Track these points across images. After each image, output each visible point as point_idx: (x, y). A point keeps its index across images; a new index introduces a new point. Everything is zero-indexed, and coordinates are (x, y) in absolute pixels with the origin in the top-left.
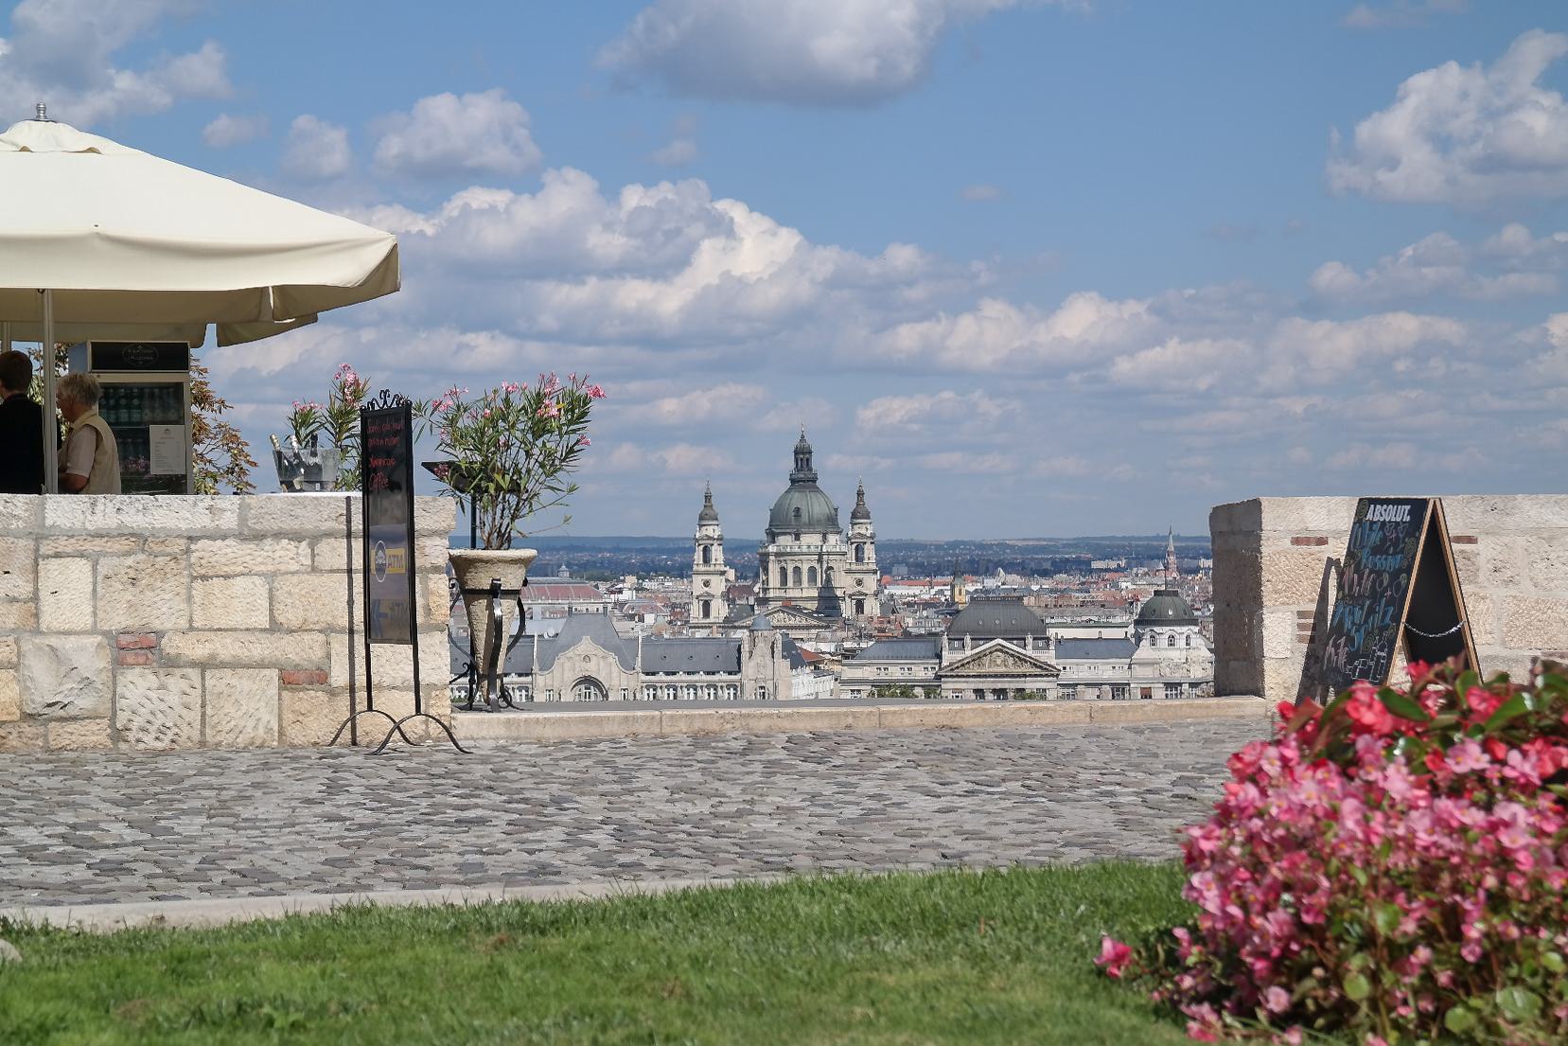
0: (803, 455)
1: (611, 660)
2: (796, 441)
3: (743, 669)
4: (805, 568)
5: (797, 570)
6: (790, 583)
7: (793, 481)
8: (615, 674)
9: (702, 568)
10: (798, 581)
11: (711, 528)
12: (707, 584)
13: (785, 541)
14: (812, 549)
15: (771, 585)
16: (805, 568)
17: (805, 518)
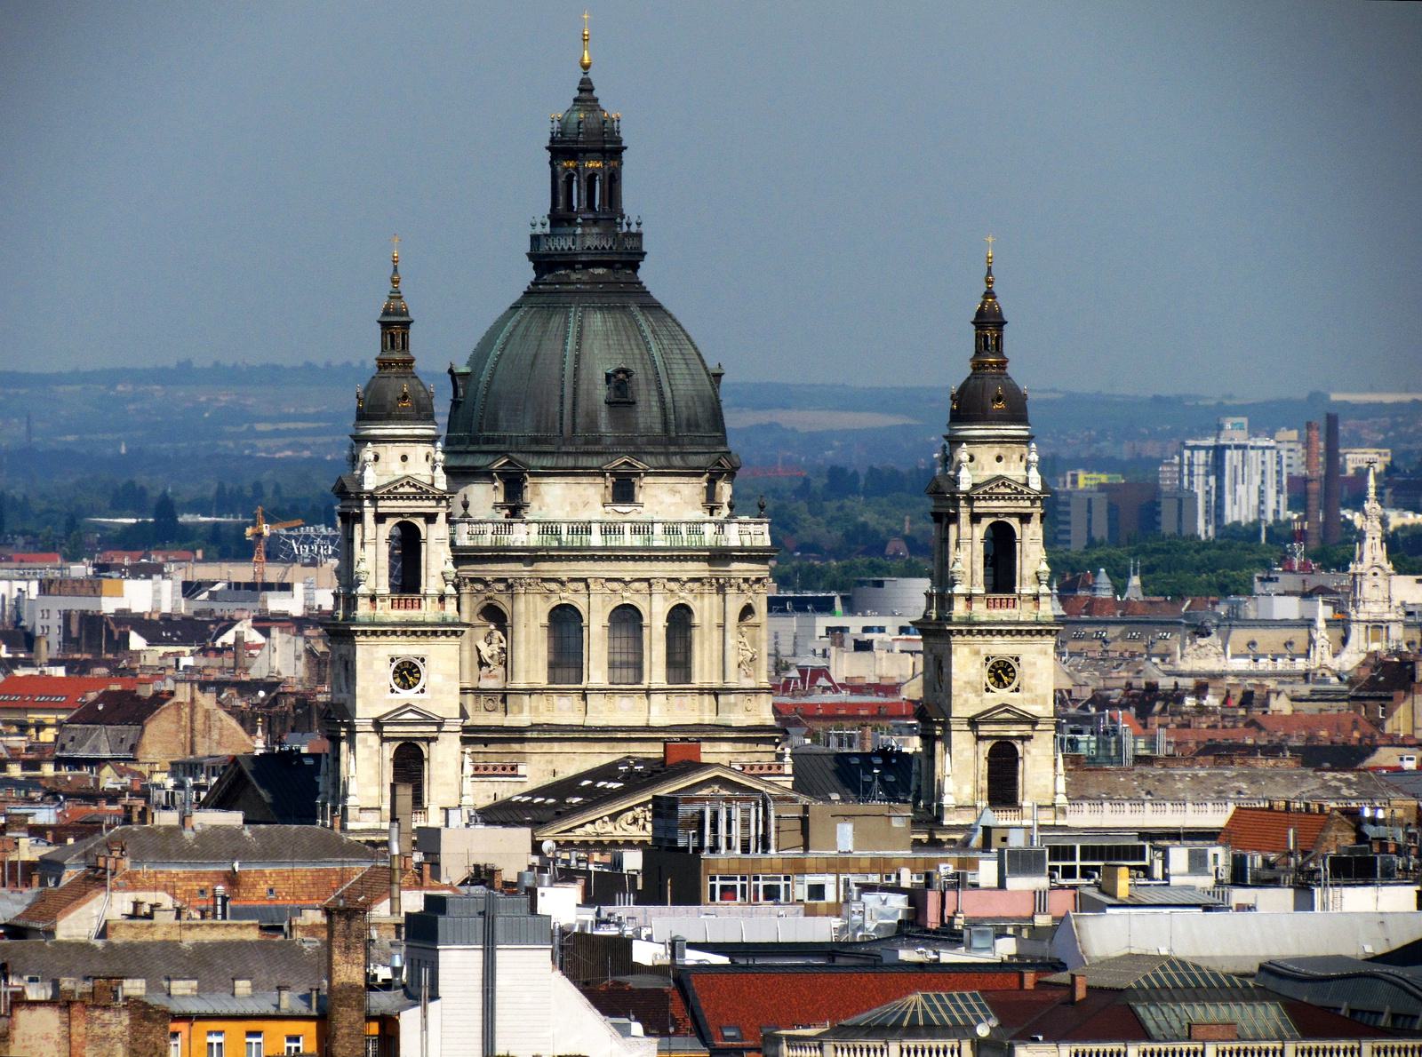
2: (558, 105)
5: (627, 619)
6: (597, 672)
7: (544, 262)
9: (388, 612)
10: (629, 666)
12: (407, 673)
14: (685, 539)
17: (647, 415)
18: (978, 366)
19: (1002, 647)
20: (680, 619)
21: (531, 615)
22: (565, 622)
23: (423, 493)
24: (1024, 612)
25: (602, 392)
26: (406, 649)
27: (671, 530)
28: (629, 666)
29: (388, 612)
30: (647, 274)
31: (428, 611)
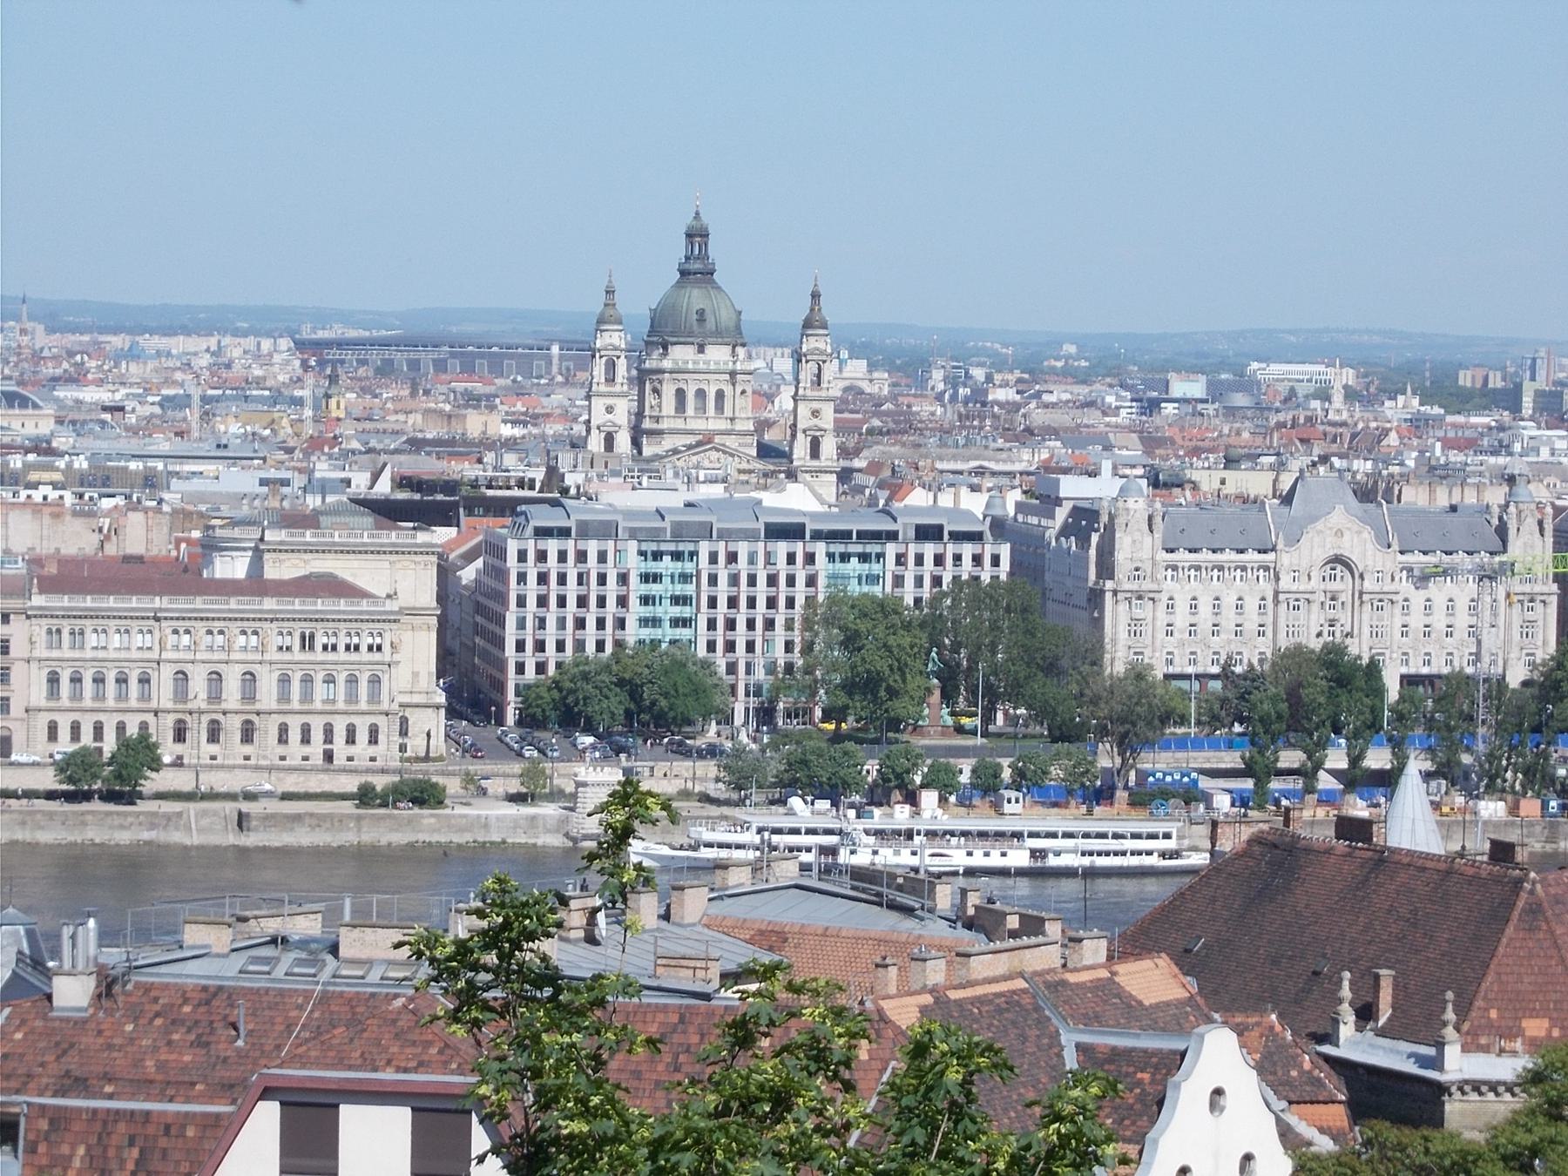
0: (697, 235)
1: (1365, 535)
2: (689, 219)
3: (1510, 548)
5: (701, 394)
6: (690, 411)
7: (684, 273)
8: (1370, 553)
9: (603, 388)
10: (701, 408)
13: (682, 354)
14: (722, 367)
15: (664, 413)
17: (710, 324)
18: (812, 310)
19: (815, 405)
20: (720, 395)
21: (668, 391)
22: (681, 394)
23: (616, 349)
24: (824, 394)
25: (695, 317)
26: (610, 401)
27: (717, 363)
28: (701, 408)
29: (603, 388)
31: (618, 388)
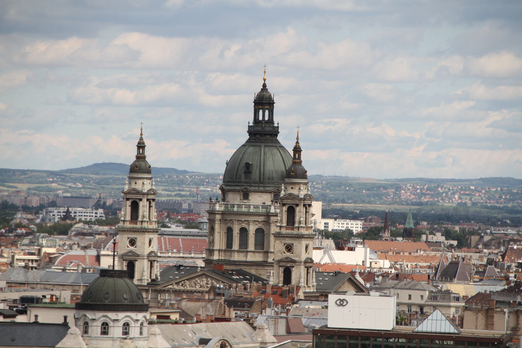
4: (252, 229)
5: (244, 232)
6: (236, 246)
7: (250, 132)
9: (128, 225)
10: (244, 244)
11: (140, 182)
12: (132, 242)
15: (217, 247)
16: (252, 229)
17: (255, 174)
27: (256, 207)
28: (244, 244)
30: (280, 138)
